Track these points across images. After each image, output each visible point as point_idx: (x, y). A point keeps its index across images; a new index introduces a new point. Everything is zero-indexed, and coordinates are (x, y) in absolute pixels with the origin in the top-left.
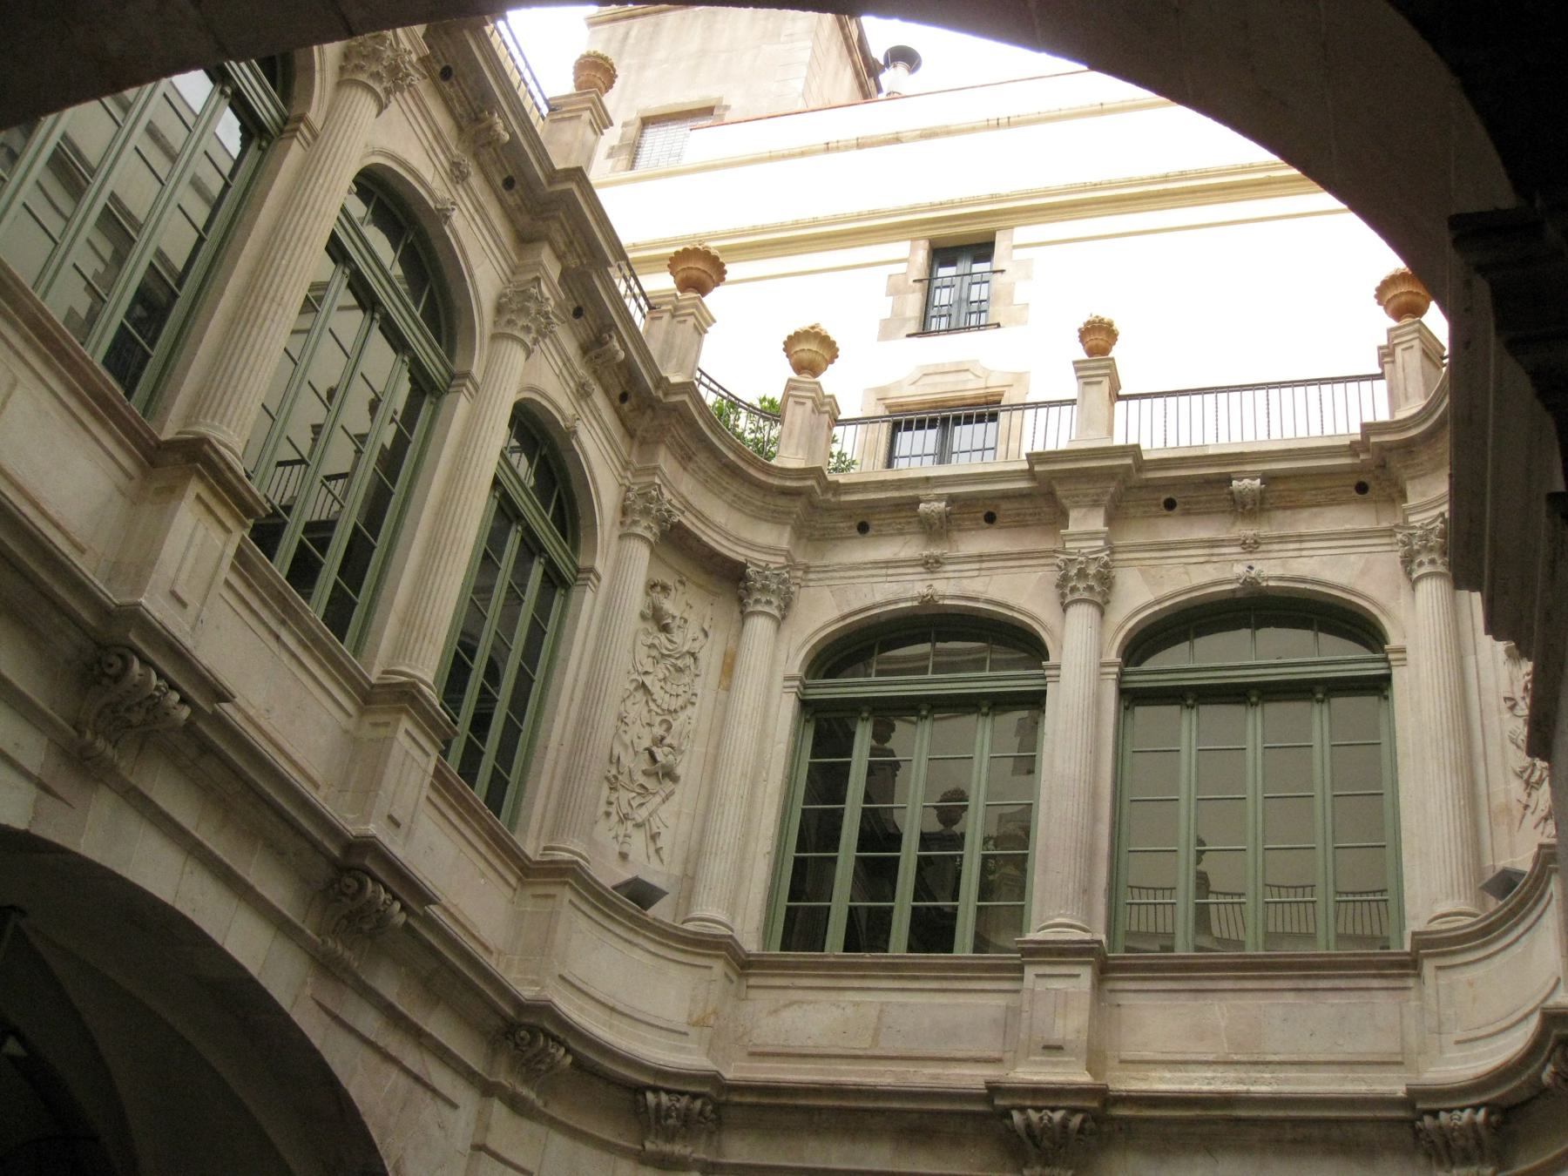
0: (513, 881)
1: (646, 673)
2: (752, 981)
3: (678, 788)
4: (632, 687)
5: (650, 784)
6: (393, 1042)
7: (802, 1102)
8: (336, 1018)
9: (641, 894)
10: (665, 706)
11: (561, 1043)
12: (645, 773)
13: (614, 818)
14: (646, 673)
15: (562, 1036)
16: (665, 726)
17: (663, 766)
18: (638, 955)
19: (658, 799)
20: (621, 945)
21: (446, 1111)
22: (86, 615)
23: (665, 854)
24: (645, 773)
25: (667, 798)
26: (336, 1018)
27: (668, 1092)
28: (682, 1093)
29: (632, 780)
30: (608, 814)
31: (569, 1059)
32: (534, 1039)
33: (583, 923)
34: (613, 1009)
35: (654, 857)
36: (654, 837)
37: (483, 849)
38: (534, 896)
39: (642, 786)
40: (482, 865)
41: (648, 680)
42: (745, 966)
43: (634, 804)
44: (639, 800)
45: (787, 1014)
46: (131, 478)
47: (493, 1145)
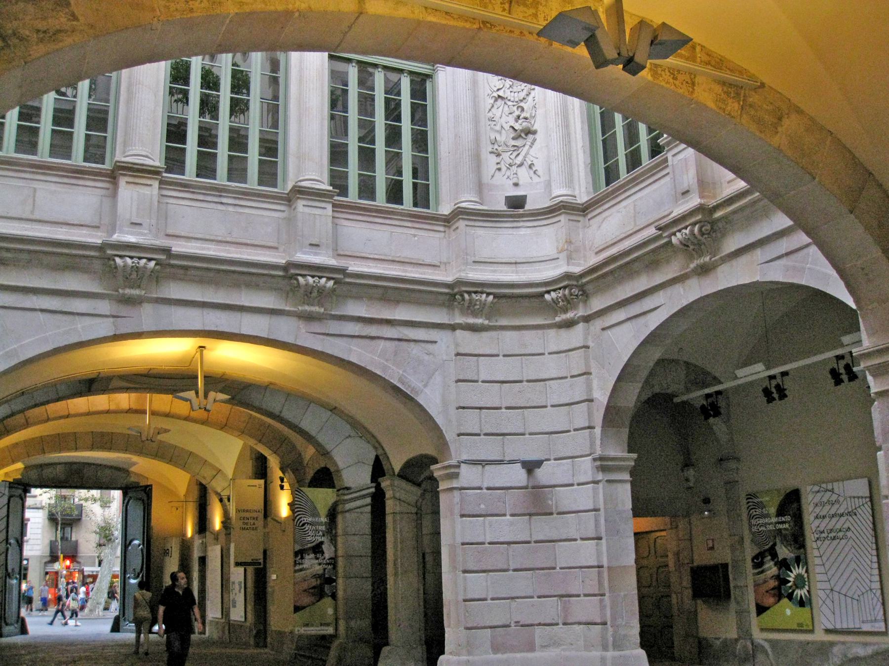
0: (442, 229)
1: (498, 90)
2: (589, 216)
3: (537, 136)
4: (492, 101)
5: (518, 143)
6: (373, 330)
7: (604, 271)
8: (328, 335)
9: (516, 203)
10: (517, 99)
11: (482, 293)
12: (513, 139)
13: (504, 169)
14: (498, 90)
15: (479, 290)
16: (520, 109)
17: (522, 131)
18: (523, 231)
19: (527, 147)
20: (510, 231)
21: (430, 347)
22: (92, 253)
23: (540, 173)
24: (513, 139)
25: (532, 144)
26: (328, 335)
27: (554, 290)
28: (560, 289)
29: (507, 146)
30: (499, 169)
31: (491, 297)
32: (462, 296)
33: (480, 232)
34: (516, 263)
35: (535, 177)
36: (531, 166)
37: (409, 224)
38: (454, 230)
39: (514, 146)
40: (413, 231)
41: (501, 93)
42: (584, 210)
43: (513, 157)
44: (515, 154)
45: (604, 225)
46: (108, 189)
47: (462, 351)
